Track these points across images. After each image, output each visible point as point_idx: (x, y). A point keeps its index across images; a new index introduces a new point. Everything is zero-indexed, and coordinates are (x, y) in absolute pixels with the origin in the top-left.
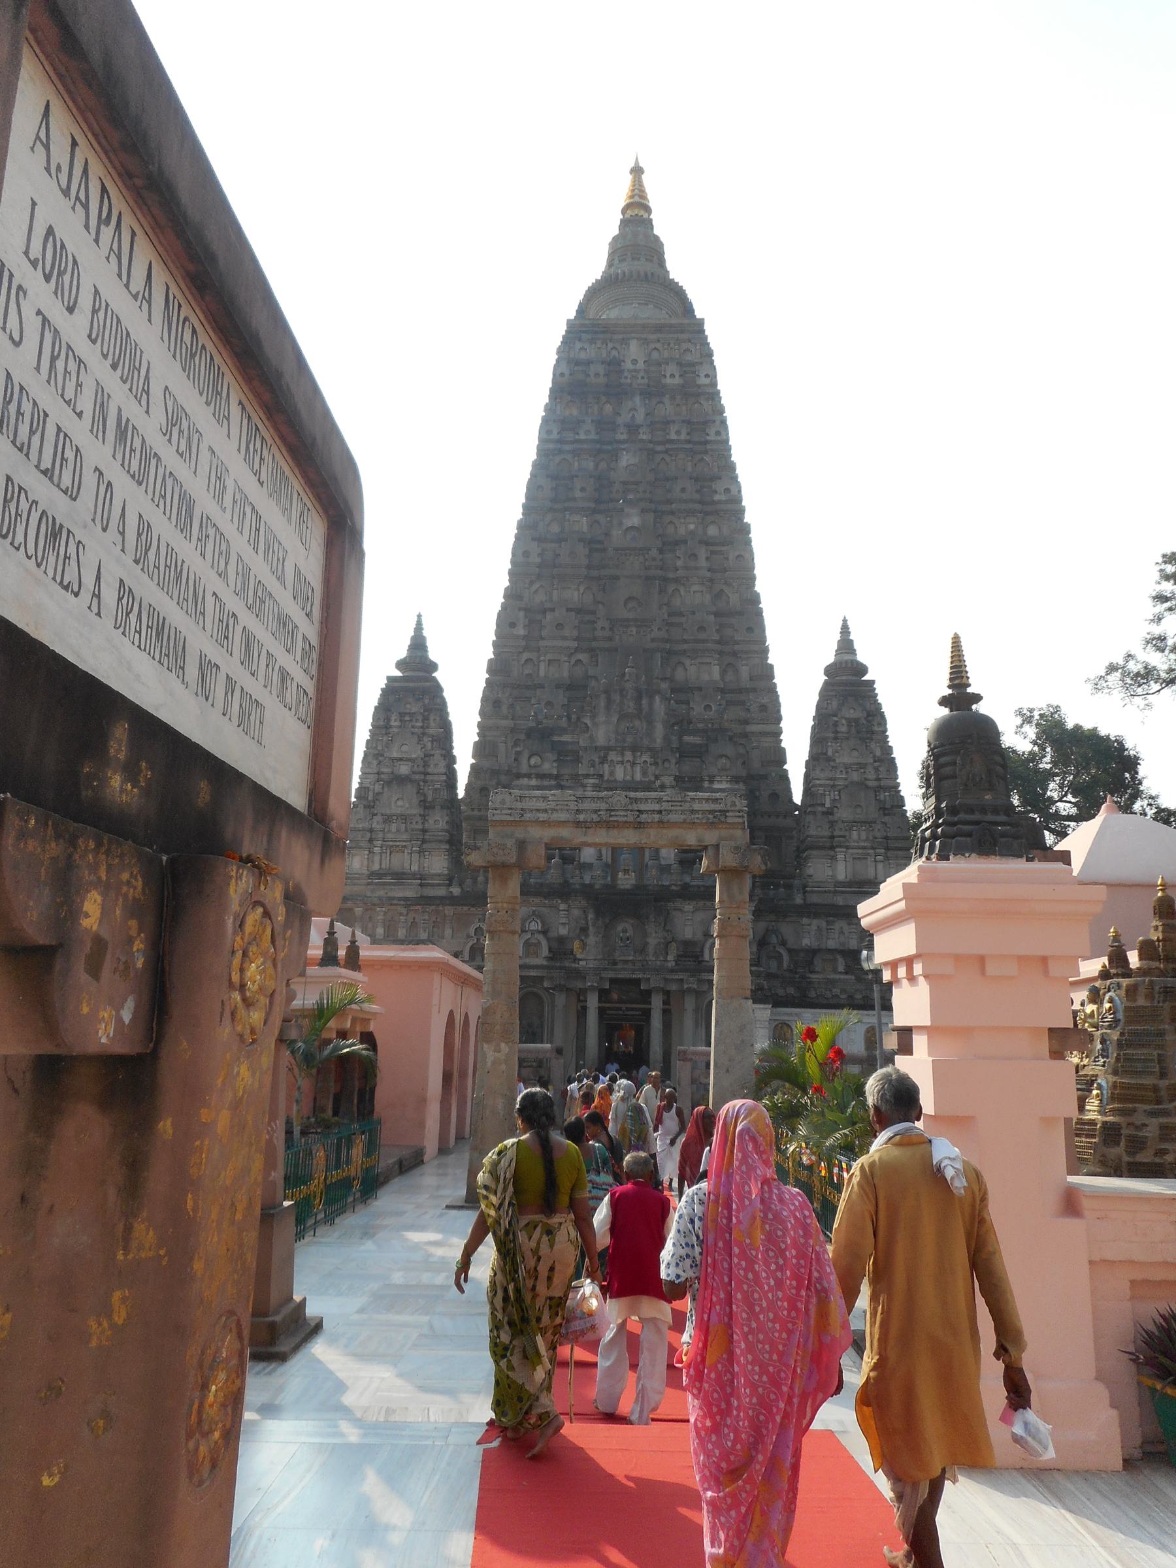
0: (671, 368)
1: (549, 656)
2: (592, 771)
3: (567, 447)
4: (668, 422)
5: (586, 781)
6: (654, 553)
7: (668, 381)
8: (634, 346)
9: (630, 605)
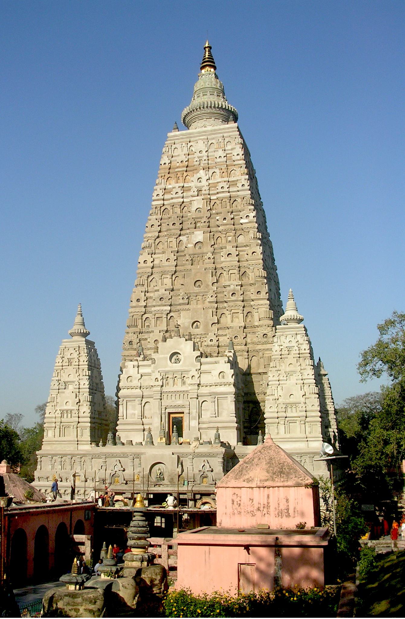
0: (221, 153)
1: (157, 316)
2: (157, 383)
3: (166, 202)
4: (218, 182)
5: (155, 389)
6: (210, 255)
7: (218, 160)
8: (201, 143)
9: (198, 284)
